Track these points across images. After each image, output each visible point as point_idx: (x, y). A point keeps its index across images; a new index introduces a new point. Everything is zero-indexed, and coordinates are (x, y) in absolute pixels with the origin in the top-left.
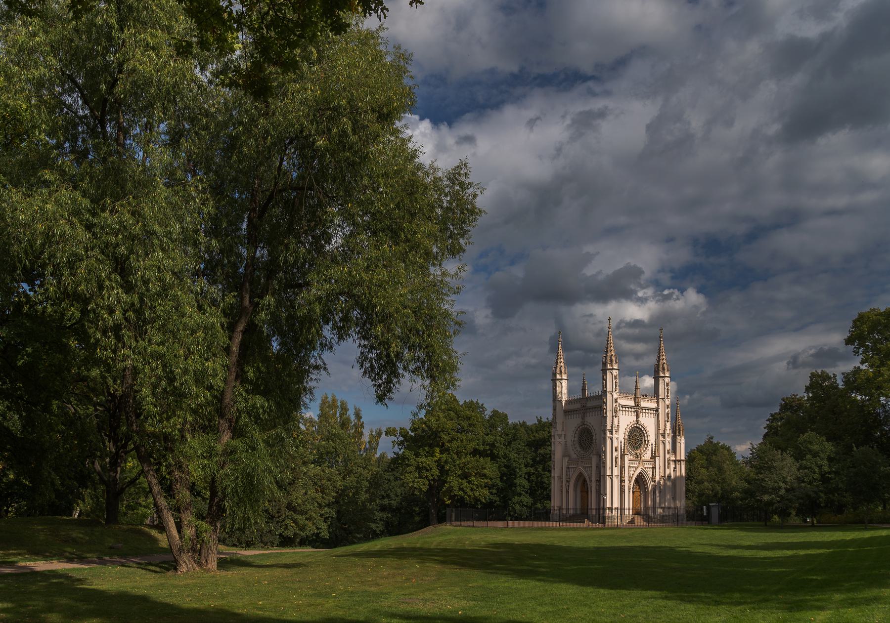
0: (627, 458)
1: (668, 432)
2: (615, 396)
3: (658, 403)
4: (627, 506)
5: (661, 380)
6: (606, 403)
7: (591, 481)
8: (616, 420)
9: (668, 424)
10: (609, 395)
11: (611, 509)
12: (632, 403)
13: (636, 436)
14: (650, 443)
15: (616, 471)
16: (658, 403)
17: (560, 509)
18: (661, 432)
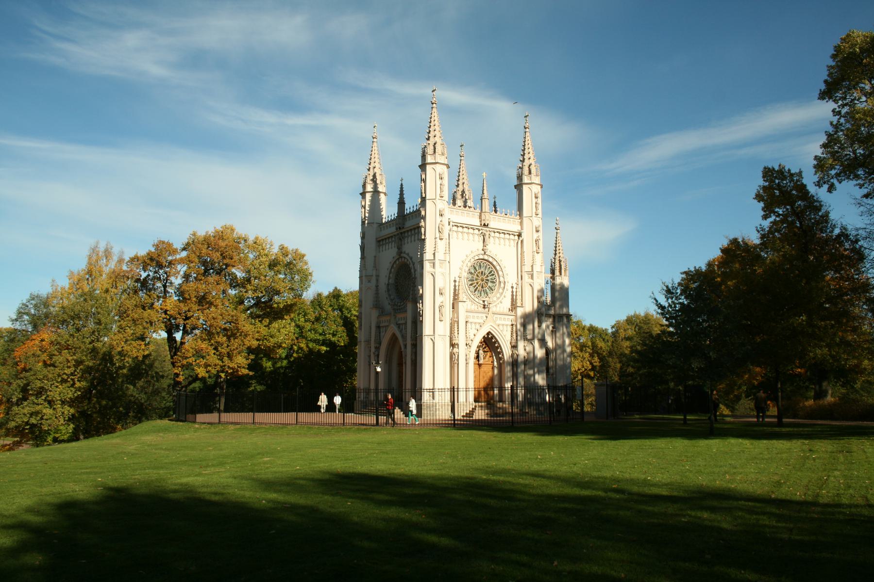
0: (462, 307)
1: (537, 268)
2: (443, 205)
3: (521, 223)
4: (462, 385)
5: (525, 187)
6: (424, 218)
7: (405, 346)
8: (441, 245)
9: (539, 258)
10: (429, 204)
11: (432, 391)
12: (477, 222)
13: (483, 276)
14: (508, 287)
15: (443, 329)
16: (521, 223)
17: (367, 391)
18: (527, 268)
